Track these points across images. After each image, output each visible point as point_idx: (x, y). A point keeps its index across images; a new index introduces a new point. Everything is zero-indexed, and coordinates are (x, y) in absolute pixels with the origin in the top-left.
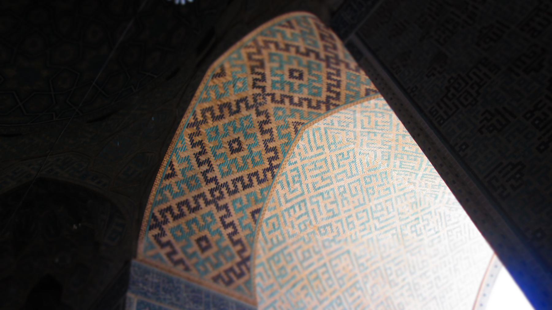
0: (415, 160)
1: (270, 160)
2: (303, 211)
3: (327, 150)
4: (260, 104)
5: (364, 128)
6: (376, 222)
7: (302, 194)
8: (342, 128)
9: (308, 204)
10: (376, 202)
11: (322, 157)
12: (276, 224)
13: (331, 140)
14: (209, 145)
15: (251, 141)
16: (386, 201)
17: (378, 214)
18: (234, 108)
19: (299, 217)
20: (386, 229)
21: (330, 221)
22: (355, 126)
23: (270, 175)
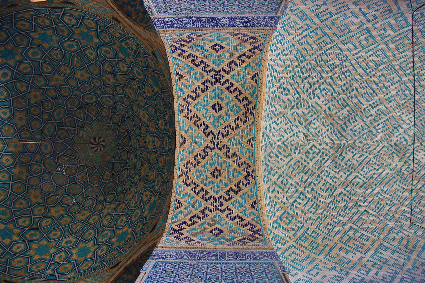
0: (356, 121)
1: (245, 170)
2: (306, 200)
3: (294, 155)
4: (218, 144)
5: (303, 124)
6: (371, 180)
7: (297, 190)
8: (291, 134)
9: (307, 194)
10: (360, 168)
11: (294, 160)
12: (289, 217)
13: (293, 148)
14: (198, 181)
15: (225, 165)
16: (368, 163)
17: (369, 174)
18: (203, 154)
19: (305, 206)
20: (385, 181)
21: (332, 197)
22: (297, 127)
23: (251, 178)
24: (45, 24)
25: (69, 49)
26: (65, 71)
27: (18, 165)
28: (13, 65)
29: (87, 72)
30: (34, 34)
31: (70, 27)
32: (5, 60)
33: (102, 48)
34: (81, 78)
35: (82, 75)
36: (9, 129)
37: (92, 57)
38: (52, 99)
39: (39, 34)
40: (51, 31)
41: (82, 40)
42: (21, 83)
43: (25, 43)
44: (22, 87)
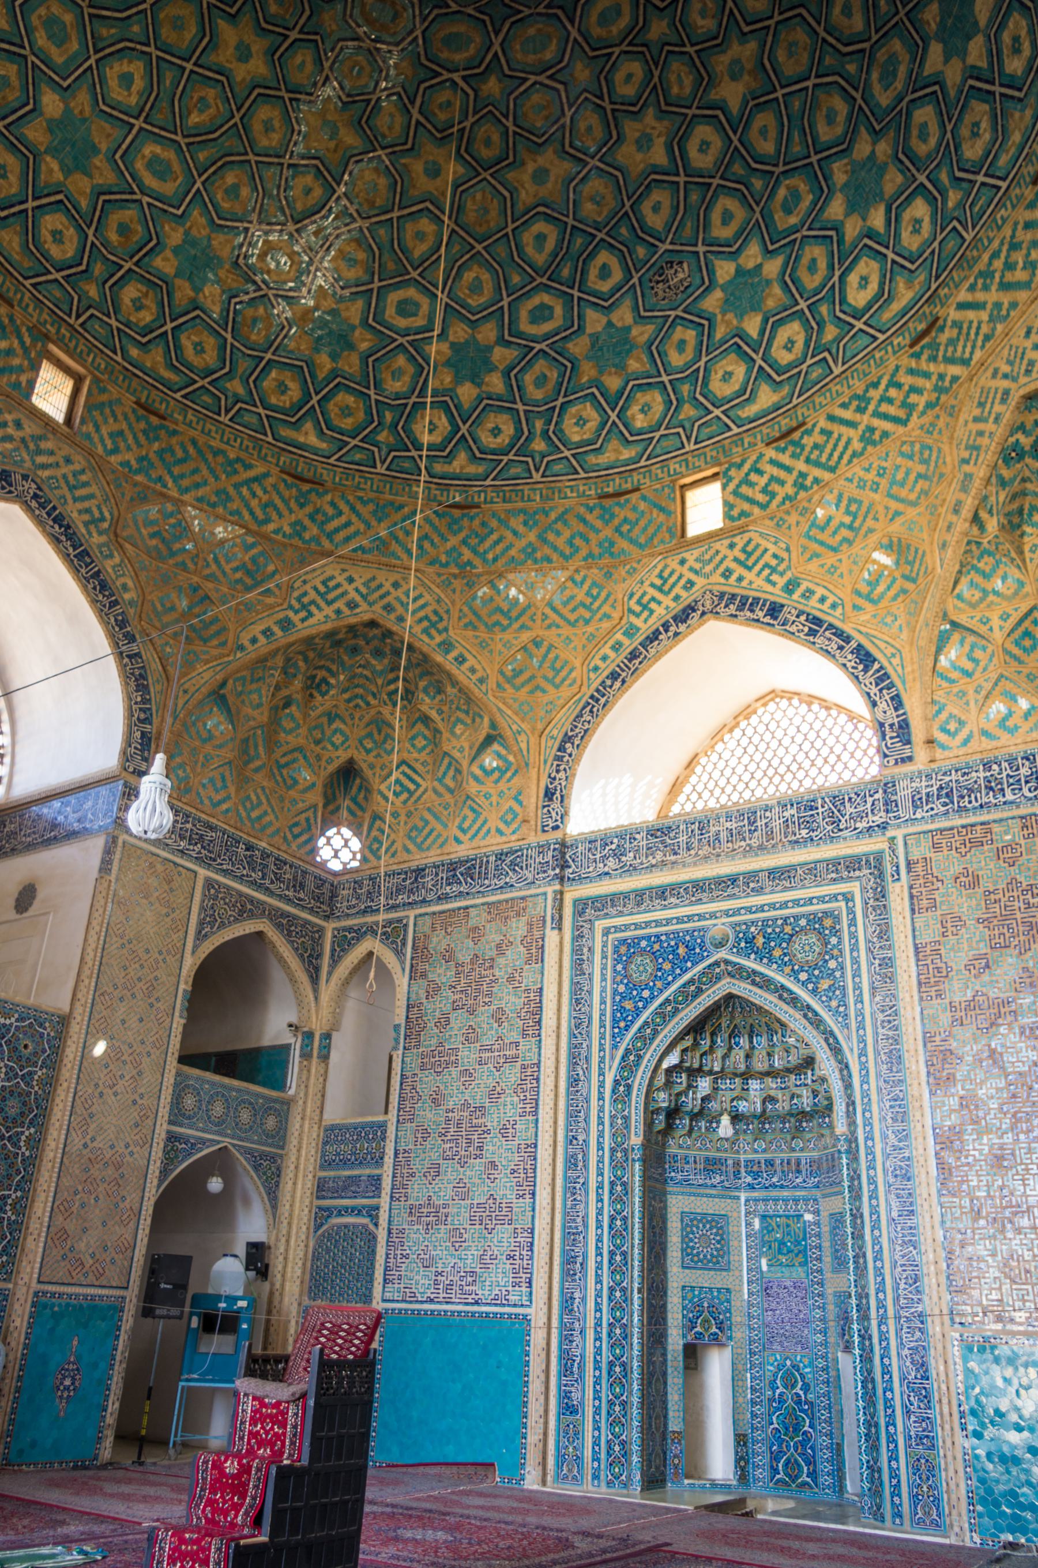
24: (146, 295)
25: (176, 167)
26: (276, 124)
27: (713, 96)
28: (360, 304)
29: (213, 44)
30: (208, 304)
31: (81, 221)
32: (357, 333)
33: (58, 57)
34: (254, 48)
35: (244, 54)
36: (592, 199)
37: (136, 68)
38: (412, 103)
39: (197, 290)
40: (158, 262)
41: (104, 147)
42: (410, 244)
43: (261, 311)
44: (420, 236)
